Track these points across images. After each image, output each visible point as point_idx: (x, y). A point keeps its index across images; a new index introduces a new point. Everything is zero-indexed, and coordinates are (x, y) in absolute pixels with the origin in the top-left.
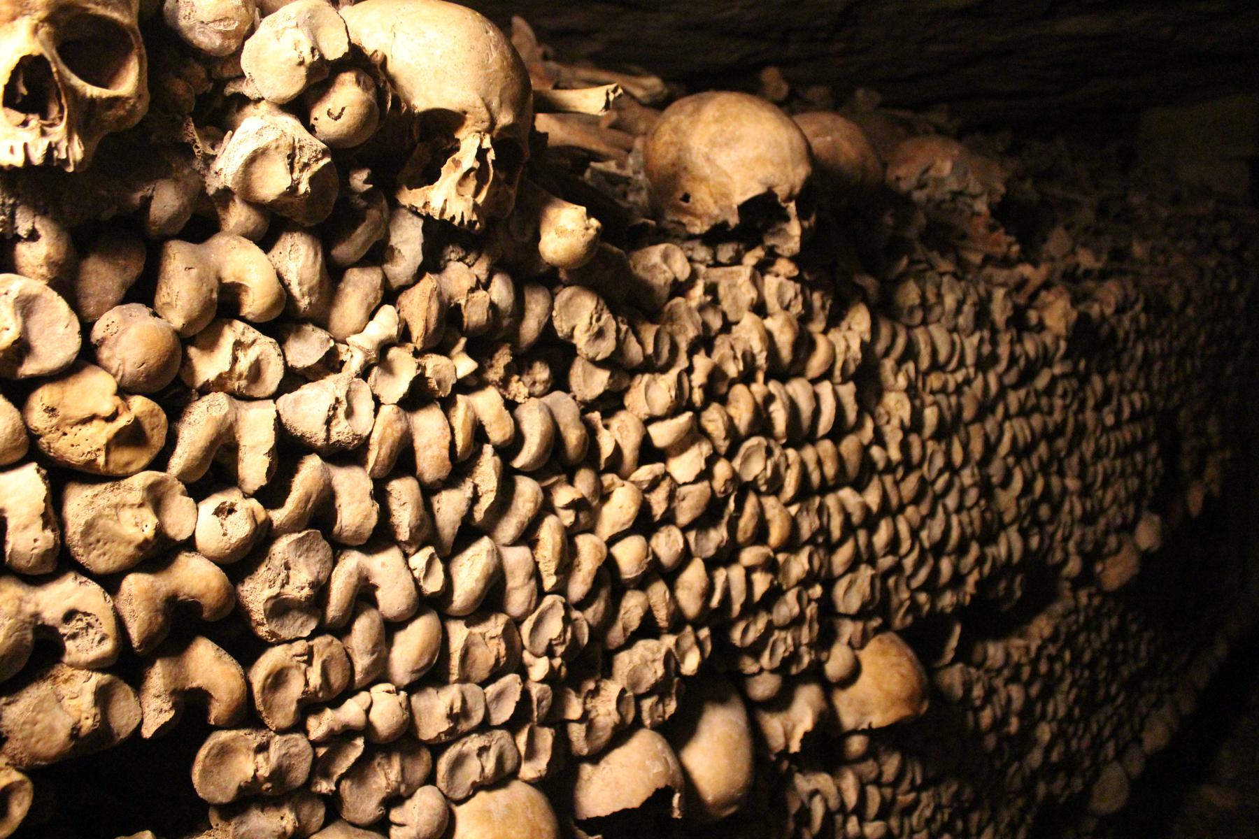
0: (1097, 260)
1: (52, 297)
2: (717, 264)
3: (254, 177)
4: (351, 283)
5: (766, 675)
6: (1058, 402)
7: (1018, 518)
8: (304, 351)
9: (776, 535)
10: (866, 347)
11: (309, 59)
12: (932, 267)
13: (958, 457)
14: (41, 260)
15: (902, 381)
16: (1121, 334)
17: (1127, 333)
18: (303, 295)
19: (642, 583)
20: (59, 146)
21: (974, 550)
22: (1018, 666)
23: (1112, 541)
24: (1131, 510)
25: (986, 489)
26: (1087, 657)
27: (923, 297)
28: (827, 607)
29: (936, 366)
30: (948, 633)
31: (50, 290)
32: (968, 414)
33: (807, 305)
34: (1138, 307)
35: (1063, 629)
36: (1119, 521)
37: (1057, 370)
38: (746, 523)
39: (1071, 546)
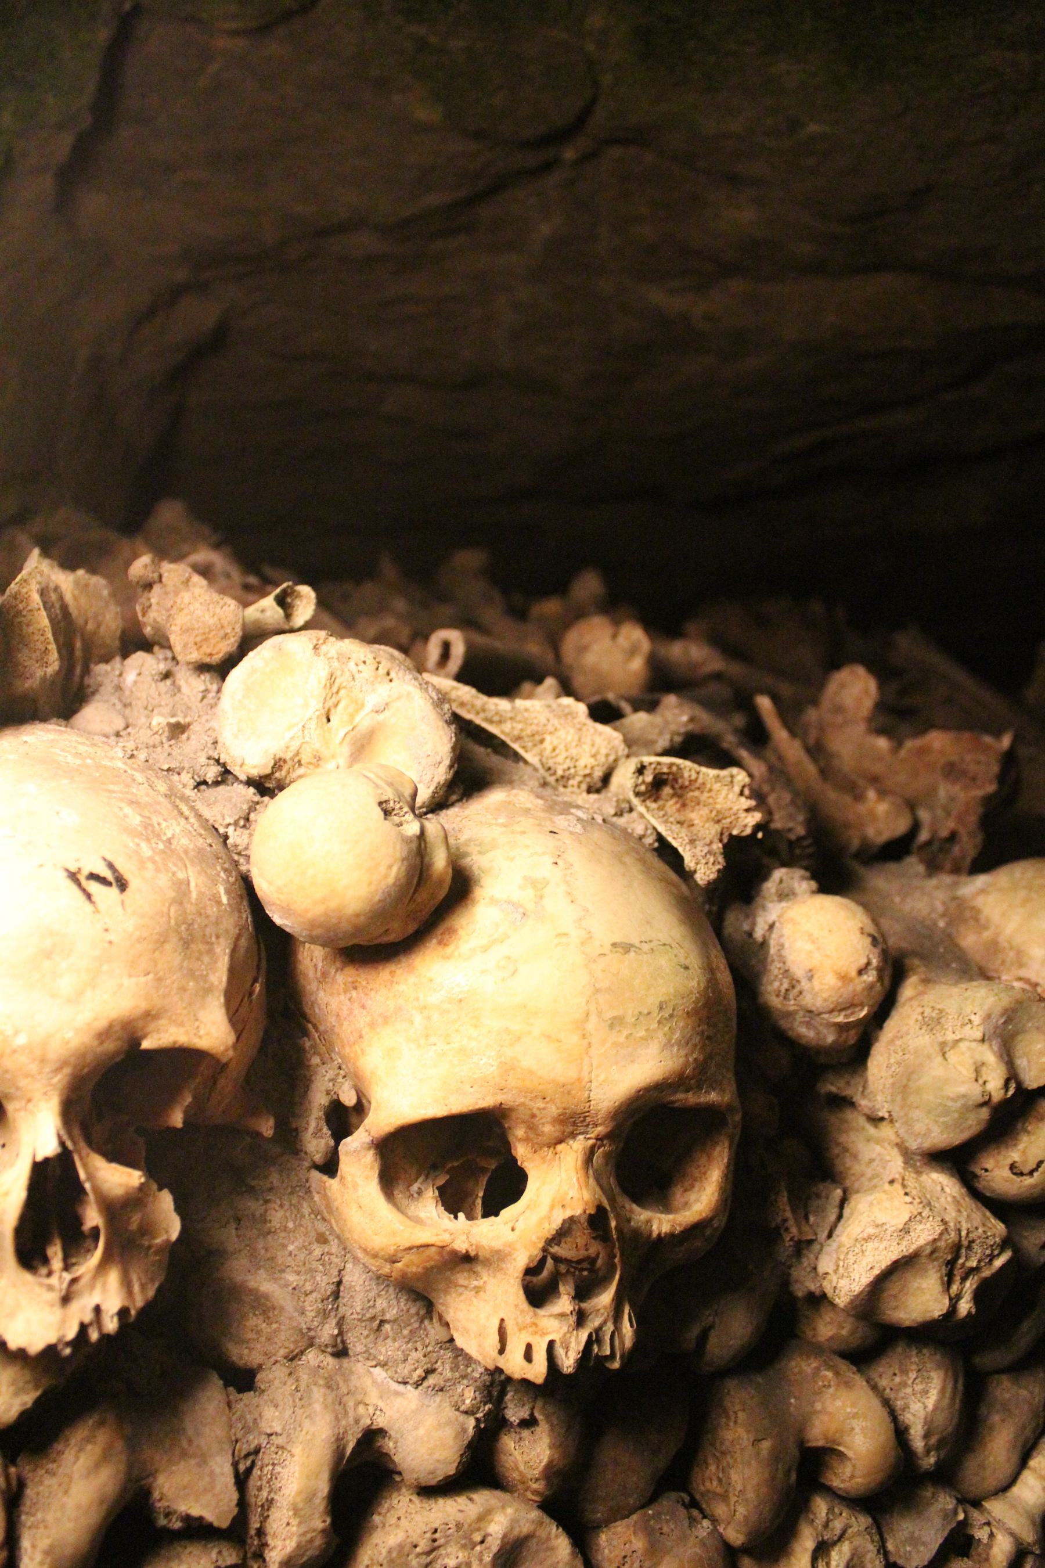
1: (549, 1534)
3: (885, 1294)
4: (998, 1406)
8: (917, 1533)
11: (997, 1096)
14: (536, 1473)
18: (928, 1452)
20: (601, 1333)
31: (547, 1519)
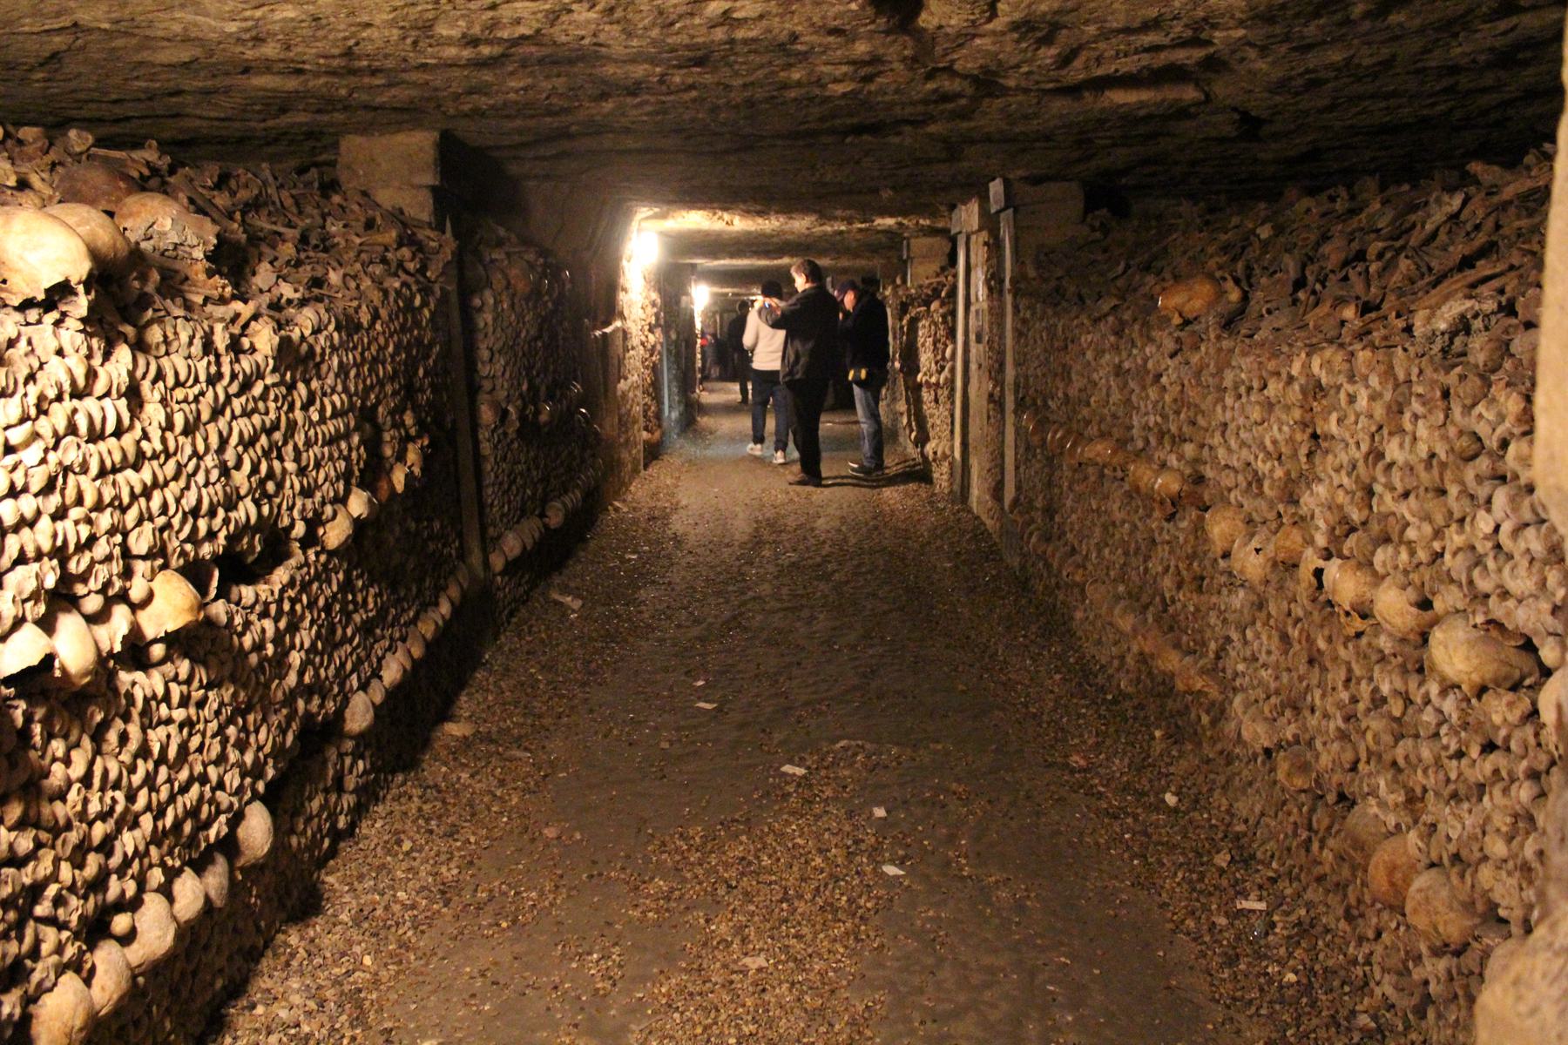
0: (296, 291)
2: (28, 324)
5: (93, 595)
6: (272, 405)
7: (251, 491)
9: (89, 500)
10: (131, 374)
12: (168, 314)
13: (201, 448)
15: (157, 396)
16: (318, 350)
17: (323, 350)
19: (16, 529)
21: (221, 513)
22: (267, 604)
23: (329, 510)
24: (341, 486)
25: (225, 471)
26: (321, 602)
27: (165, 336)
28: (126, 554)
29: (178, 384)
30: (211, 576)
32: (205, 416)
33: (90, 348)
34: (331, 327)
35: (298, 578)
36: (332, 494)
37: (269, 381)
38: (71, 494)
39: (296, 514)
